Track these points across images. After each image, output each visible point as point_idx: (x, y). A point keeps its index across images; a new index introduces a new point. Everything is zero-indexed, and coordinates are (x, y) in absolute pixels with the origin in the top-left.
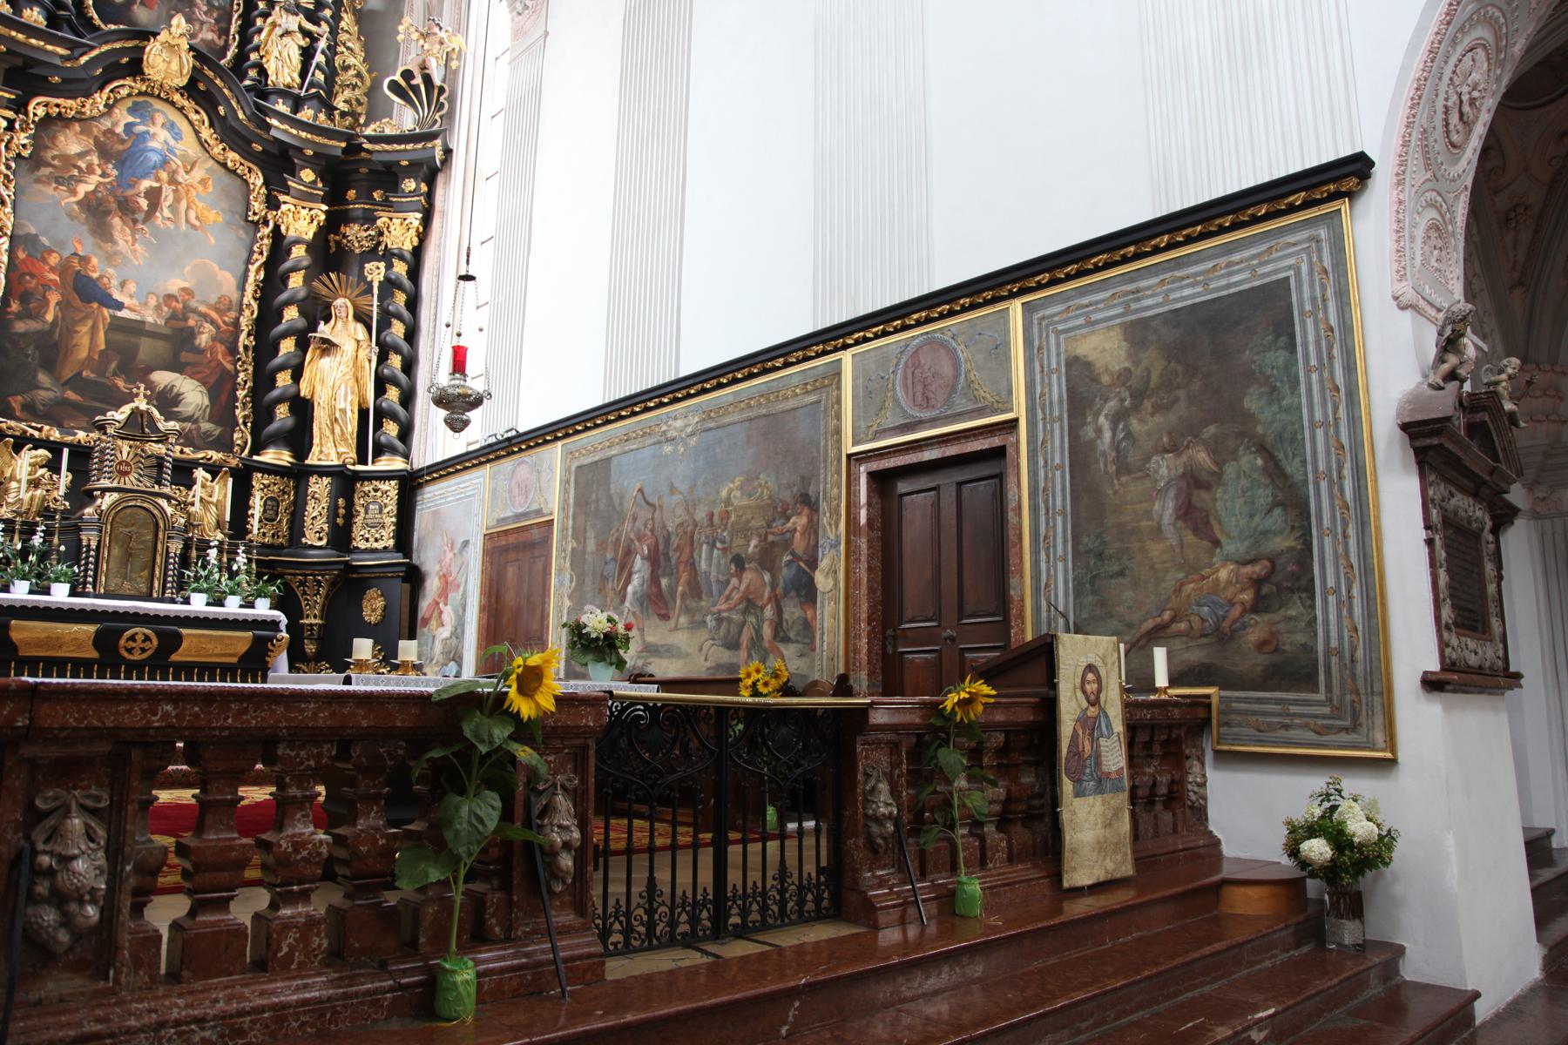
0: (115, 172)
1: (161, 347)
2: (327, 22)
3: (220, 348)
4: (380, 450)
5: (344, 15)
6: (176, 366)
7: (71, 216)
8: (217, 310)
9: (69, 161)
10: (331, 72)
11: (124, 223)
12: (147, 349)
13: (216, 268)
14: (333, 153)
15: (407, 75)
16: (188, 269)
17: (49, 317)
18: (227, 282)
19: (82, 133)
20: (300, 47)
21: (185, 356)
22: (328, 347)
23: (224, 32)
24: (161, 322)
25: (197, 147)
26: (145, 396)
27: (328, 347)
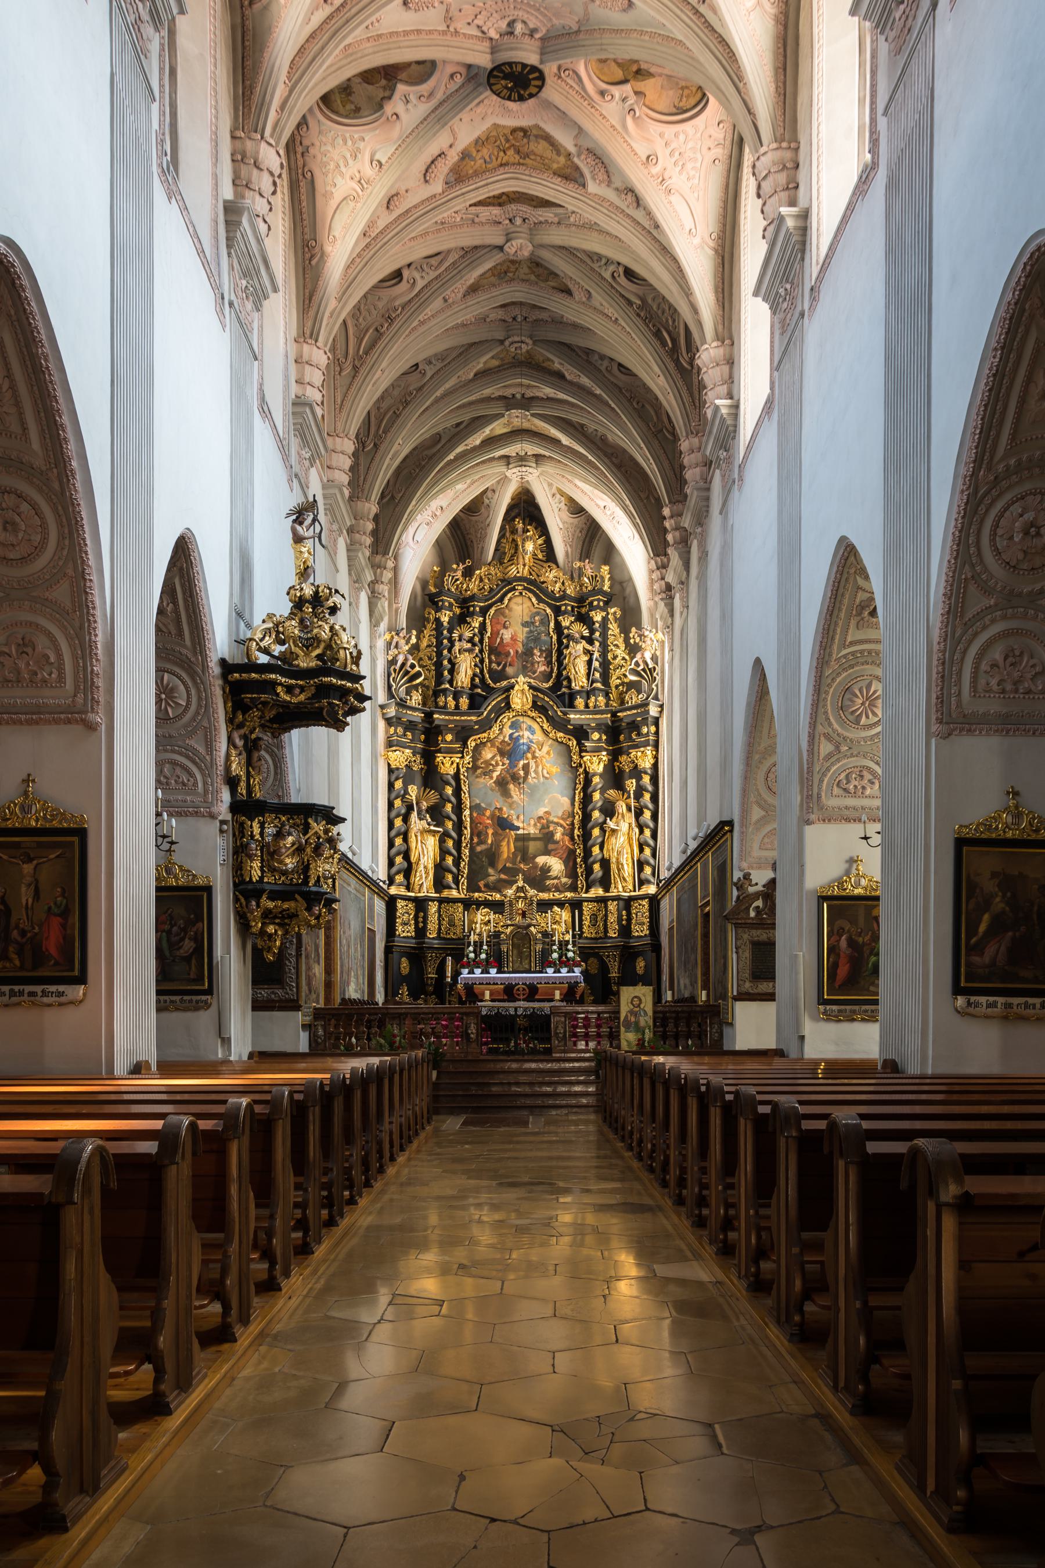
1: (539, 844)
3: (567, 838)
5: (610, 626)
6: (547, 852)
7: (492, 790)
8: (563, 819)
9: (487, 763)
10: (605, 665)
12: (533, 847)
15: (637, 664)
17: (490, 842)
18: (566, 801)
21: (551, 847)
24: (537, 832)
27: (614, 831)
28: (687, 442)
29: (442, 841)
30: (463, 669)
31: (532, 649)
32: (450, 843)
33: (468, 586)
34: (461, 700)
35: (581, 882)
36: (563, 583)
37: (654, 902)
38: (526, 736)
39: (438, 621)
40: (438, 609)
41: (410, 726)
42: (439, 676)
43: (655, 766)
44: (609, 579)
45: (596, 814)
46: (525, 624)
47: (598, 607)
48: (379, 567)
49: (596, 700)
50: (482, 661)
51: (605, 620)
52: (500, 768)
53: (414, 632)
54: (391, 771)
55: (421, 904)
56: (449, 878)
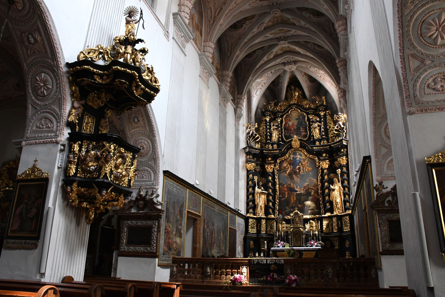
0: (292, 167)
2: (322, 121)
3: (316, 194)
4: (346, 209)
5: (327, 117)
9: (285, 168)
11: (295, 176)
12: (303, 198)
13: (312, 178)
14: (327, 149)
15: (337, 127)
16: (307, 180)
17: (286, 197)
18: (315, 180)
19: (286, 162)
20: (318, 129)
22: (334, 190)
23: (306, 132)
25: (305, 157)
26: (297, 209)
27: (334, 190)
28: (337, 24)
29: (268, 197)
30: (274, 135)
31: (300, 127)
32: (271, 198)
33: (276, 109)
34: (274, 146)
35: (322, 211)
36: (310, 105)
37: (351, 216)
38: (299, 158)
39: (266, 120)
40: (265, 116)
41: (254, 155)
42: (266, 137)
43: (348, 164)
44: (325, 101)
45: (326, 184)
46: (297, 119)
47: (322, 110)
48: (239, 99)
49: (324, 142)
50: (282, 133)
51: (325, 115)
52: (289, 169)
53: (256, 124)
54: (248, 171)
55: (259, 220)
56: (271, 211)
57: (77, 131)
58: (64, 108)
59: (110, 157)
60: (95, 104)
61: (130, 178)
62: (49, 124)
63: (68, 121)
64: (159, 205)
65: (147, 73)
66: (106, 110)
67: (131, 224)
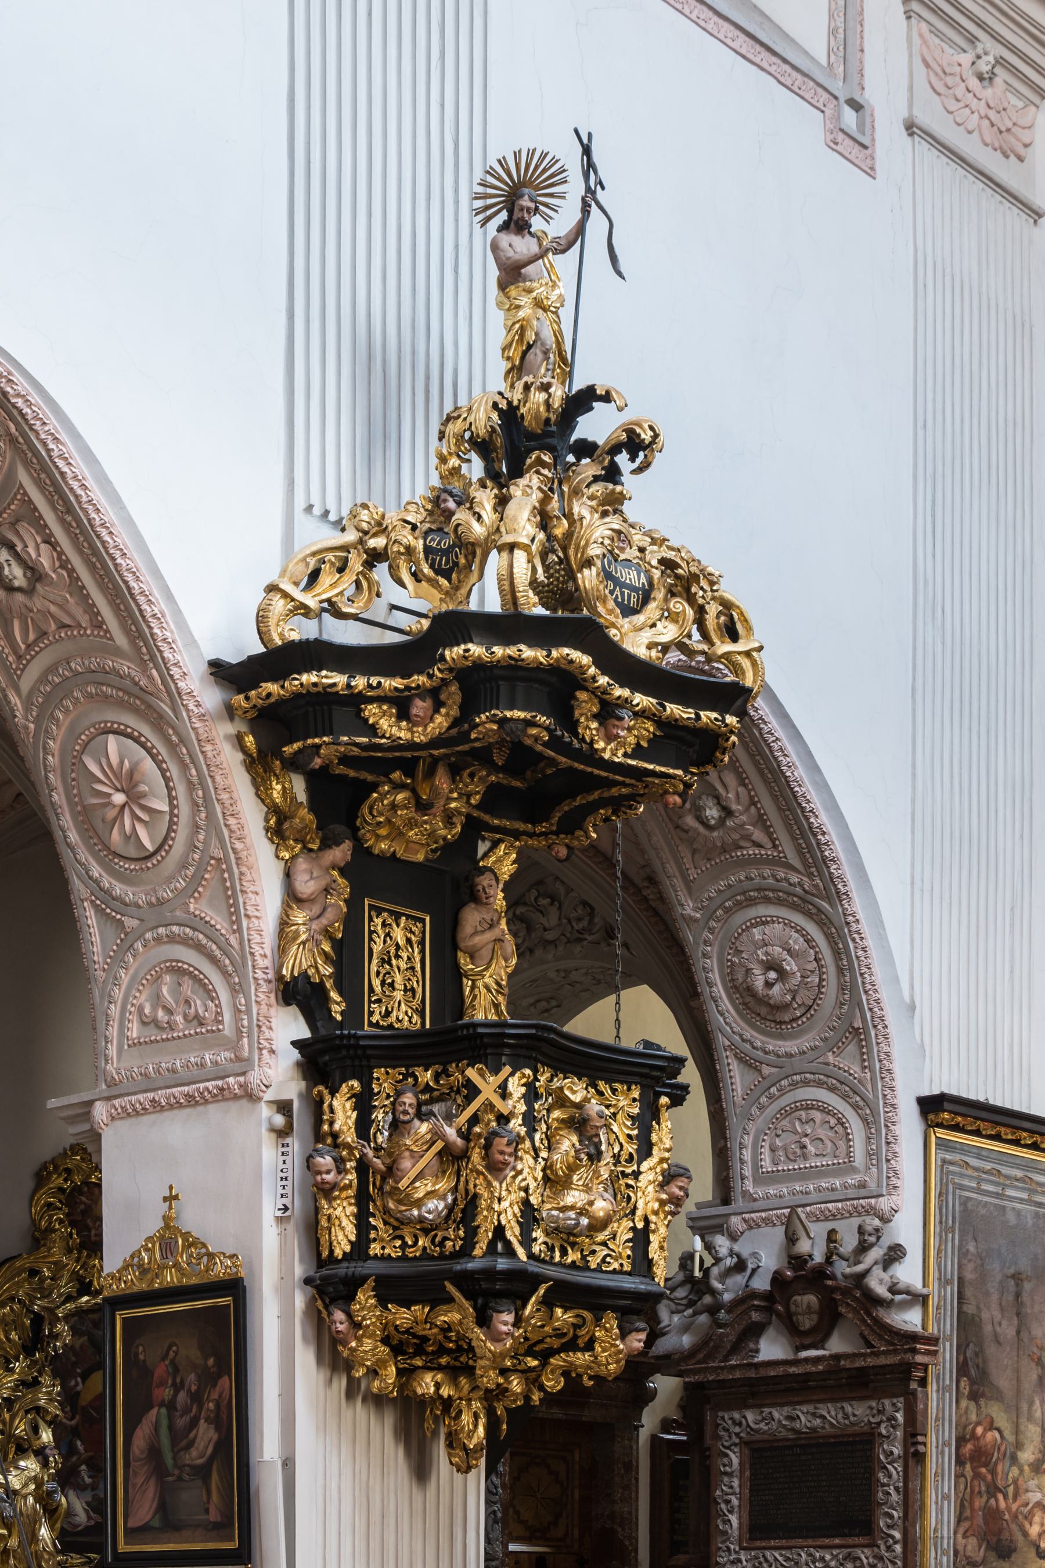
57: (339, 1018)
58: (251, 912)
59: (509, 1144)
60: (409, 841)
61: (640, 1225)
62: (198, 1002)
63: (280, 978)
64: (905, 1306)
65: (666, 600)
66: (482, 847)
67: (762, 1425)
